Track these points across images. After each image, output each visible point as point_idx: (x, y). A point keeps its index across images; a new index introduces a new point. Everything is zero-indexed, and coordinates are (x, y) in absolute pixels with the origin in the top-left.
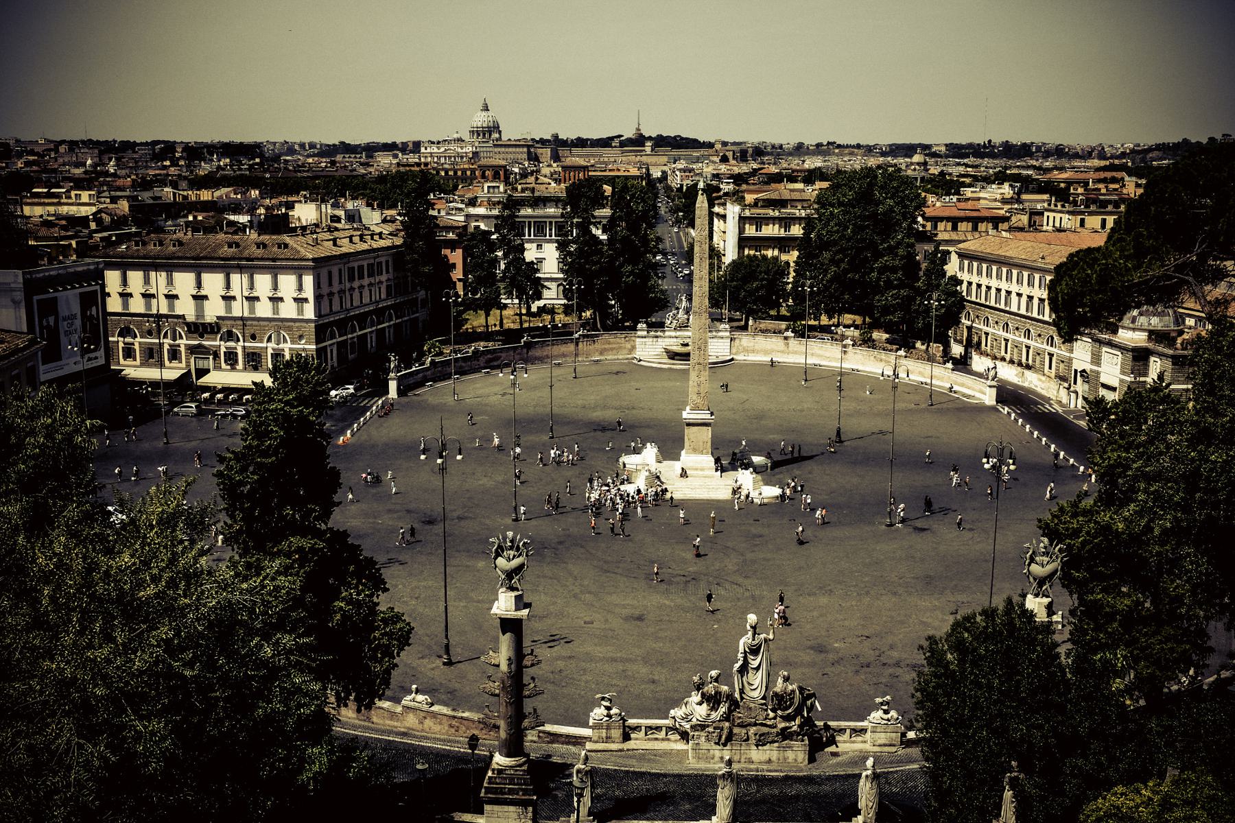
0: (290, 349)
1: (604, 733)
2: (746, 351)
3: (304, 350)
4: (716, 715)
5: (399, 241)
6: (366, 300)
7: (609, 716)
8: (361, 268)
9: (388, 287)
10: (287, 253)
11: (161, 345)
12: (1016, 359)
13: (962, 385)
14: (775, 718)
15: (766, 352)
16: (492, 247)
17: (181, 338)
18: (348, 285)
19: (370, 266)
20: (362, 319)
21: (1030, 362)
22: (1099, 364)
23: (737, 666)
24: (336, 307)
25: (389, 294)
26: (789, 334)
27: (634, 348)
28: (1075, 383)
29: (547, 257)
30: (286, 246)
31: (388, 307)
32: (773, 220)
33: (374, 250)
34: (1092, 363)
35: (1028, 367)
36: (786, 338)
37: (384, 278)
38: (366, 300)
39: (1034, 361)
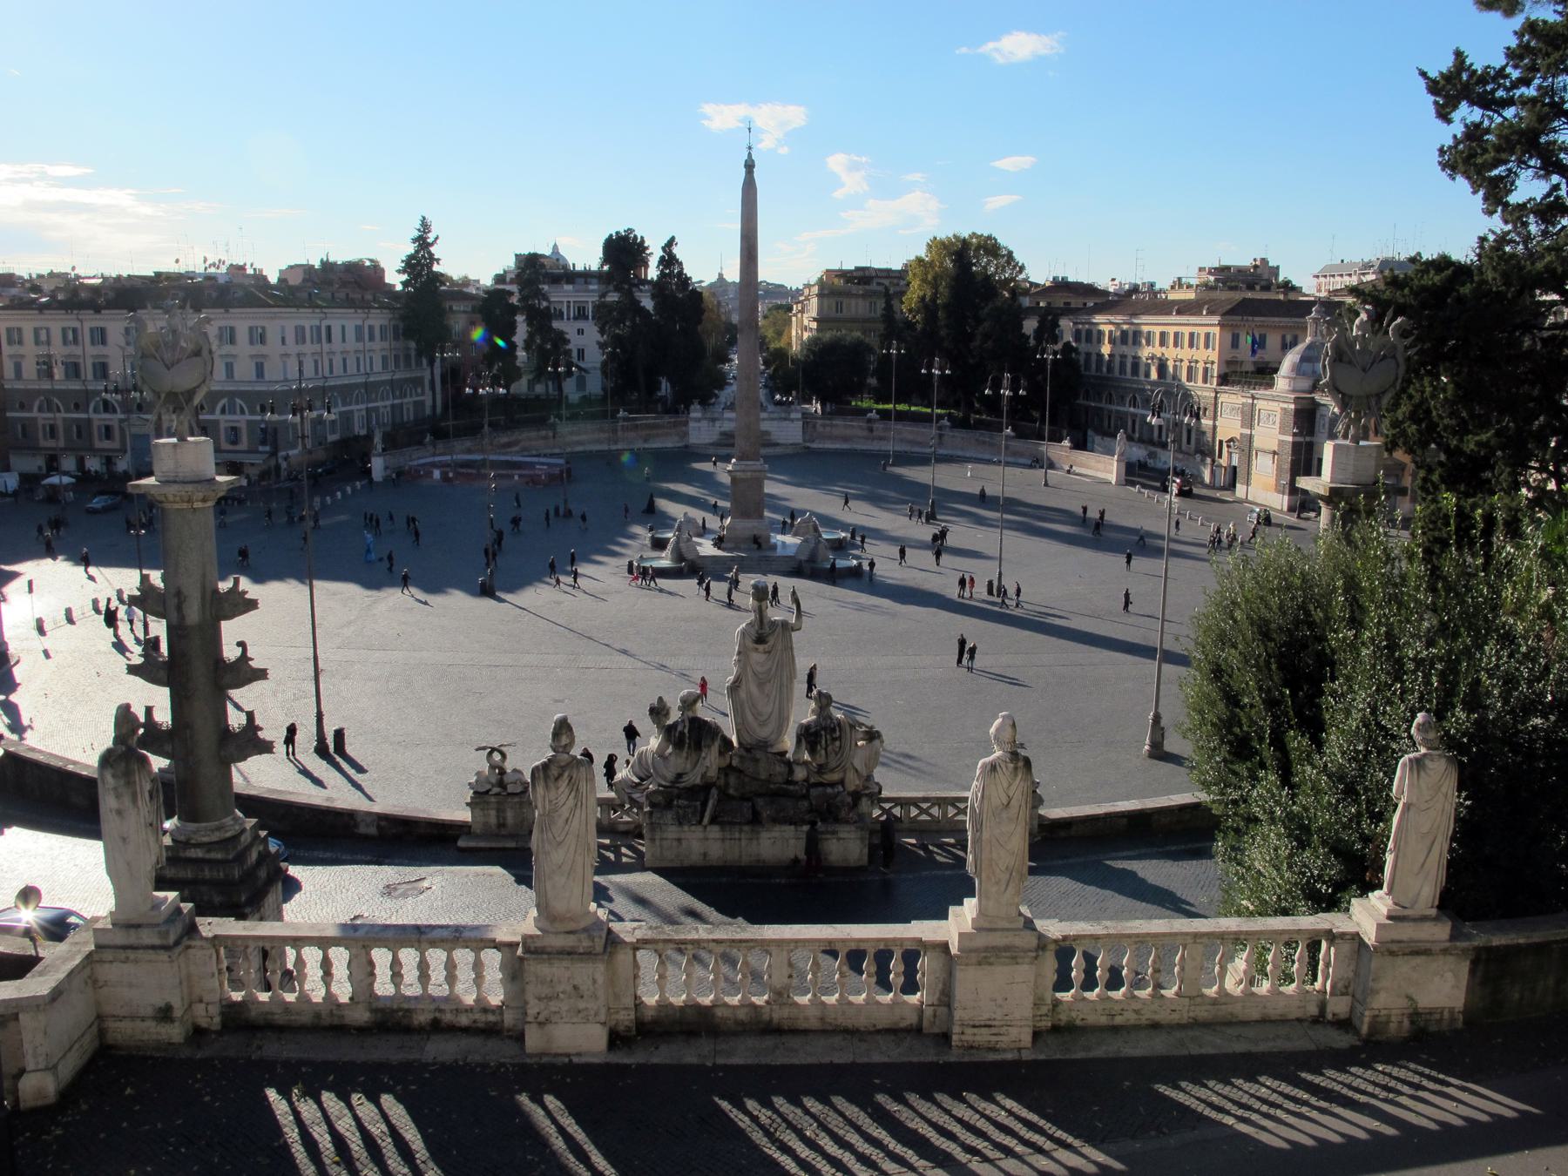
1: (493, 820)
4: (694, 778)
6: (352, 368)
7: (501, 784)
9: (384, 359)
11: (89, 421)
12: (1145, 437)
13: (1082, 465)
14: (806, 780)
15: (845, 439)
16: (514, 310)
17: (115, 411)
19: (359, 329)
20: (346, 392)
22: (1251, 427)
23: (731, 678)
25: (385, 366)
27: (686, 434)
29: (586, 340)
31: (383, 382)
32: (857, 296)
36: (869, 421)
38: (352, 368)
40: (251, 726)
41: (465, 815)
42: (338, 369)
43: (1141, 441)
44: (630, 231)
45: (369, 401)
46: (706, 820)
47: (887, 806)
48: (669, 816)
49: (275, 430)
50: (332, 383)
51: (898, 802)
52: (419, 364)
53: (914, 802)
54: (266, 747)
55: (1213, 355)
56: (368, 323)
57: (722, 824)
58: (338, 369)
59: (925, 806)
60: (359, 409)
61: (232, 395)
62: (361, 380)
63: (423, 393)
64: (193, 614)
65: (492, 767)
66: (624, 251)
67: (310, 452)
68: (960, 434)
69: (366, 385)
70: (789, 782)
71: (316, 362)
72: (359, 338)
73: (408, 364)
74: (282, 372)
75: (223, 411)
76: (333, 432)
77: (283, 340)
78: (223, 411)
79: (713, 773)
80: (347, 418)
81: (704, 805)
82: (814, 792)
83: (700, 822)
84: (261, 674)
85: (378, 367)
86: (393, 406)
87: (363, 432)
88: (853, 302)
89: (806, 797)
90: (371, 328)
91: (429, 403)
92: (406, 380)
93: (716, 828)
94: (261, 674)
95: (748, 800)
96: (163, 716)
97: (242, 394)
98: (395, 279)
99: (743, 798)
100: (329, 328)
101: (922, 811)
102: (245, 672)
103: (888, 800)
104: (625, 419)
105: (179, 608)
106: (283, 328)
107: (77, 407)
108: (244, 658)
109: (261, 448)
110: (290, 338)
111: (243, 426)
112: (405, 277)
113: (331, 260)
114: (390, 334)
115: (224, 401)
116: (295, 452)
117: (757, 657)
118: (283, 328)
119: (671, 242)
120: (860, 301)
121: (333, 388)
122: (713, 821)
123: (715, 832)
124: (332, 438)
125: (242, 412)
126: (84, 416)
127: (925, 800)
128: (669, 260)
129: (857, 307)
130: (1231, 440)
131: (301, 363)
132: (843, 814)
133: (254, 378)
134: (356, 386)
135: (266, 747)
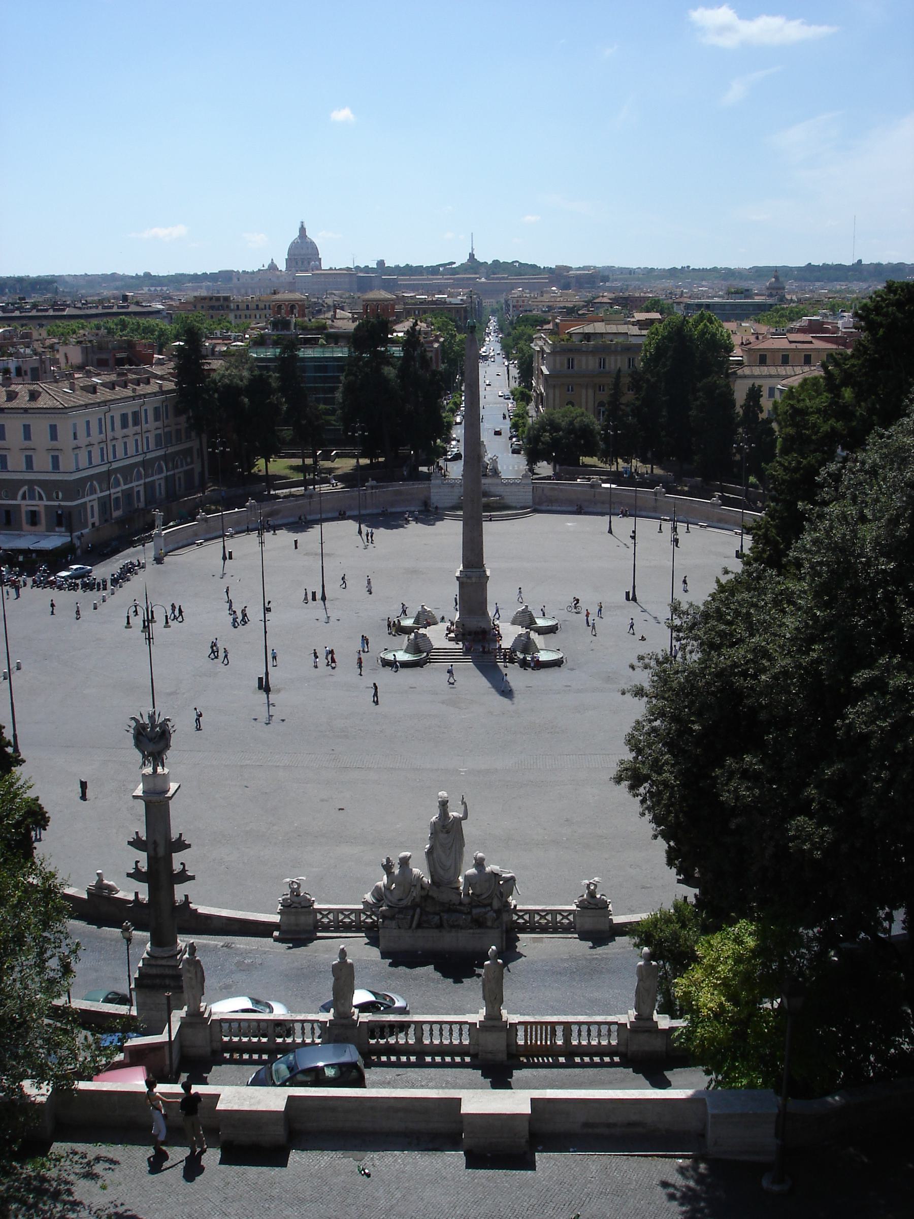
0: (46, 506)
3: (59, 506)
5: (170, 385)
8: (124, 417)
9: (158, 437)
10: (42, 403)
18: (110, 435)
20: (127, 472)
24: (96, 459)
33: (145, 396)
38: (131, 450)
41: (276, 918)
42: (120, 453)
45: (146, 476)
46: (414, 925)
47: (521, 914)
48: (393, 924)
49: (70, 514)
50: (115, 466)
57: (423, 928)
58: (120, 453)
60: (137, 485)
61: (31, 483)
62: (139, 459)
63: (192, 462)
64: (161, 851)
65: (292, 892)
67: (98, 529)
69: (144, 463)
71: (102, 449)
72: (136, 423)
74: (75, 465)
75: (24, 498)
76: (117, 508)
77: (75, 434)
78: (24, 498)
79: (418, 900)
80: (128, 494)
81: (413, 917)
82: (475, 911)
83: (410, 927)
86: (167, 478)
87: (142, 505)
88: (584, 359)
89: (470, 913)
92: (177, 453)
93: (420, 931)
94: (192, 878)
95: (438, 914)
96: (144, 897)
97: (42, 483)
99: (435, 914)
100: (112, 417)
101: (542, 917)
102: (183, 877)
103: (521, 911)
104: (372, 487)
105: (155, 849)
106: (75, 425)
108: (184, 870)
109: (57, 529)
110: (82, 433)
111: (42, 511)
115: (25, 488)
116: (87, 530)
117: (442, 836)
118: (75, 425)
121: (116, 470)
122: (419, 926)
123: (420, 933)
124: (116, 514)
125: (41, 498)
129: (588, 363)
131: (90, 452)
133: (50, 469)
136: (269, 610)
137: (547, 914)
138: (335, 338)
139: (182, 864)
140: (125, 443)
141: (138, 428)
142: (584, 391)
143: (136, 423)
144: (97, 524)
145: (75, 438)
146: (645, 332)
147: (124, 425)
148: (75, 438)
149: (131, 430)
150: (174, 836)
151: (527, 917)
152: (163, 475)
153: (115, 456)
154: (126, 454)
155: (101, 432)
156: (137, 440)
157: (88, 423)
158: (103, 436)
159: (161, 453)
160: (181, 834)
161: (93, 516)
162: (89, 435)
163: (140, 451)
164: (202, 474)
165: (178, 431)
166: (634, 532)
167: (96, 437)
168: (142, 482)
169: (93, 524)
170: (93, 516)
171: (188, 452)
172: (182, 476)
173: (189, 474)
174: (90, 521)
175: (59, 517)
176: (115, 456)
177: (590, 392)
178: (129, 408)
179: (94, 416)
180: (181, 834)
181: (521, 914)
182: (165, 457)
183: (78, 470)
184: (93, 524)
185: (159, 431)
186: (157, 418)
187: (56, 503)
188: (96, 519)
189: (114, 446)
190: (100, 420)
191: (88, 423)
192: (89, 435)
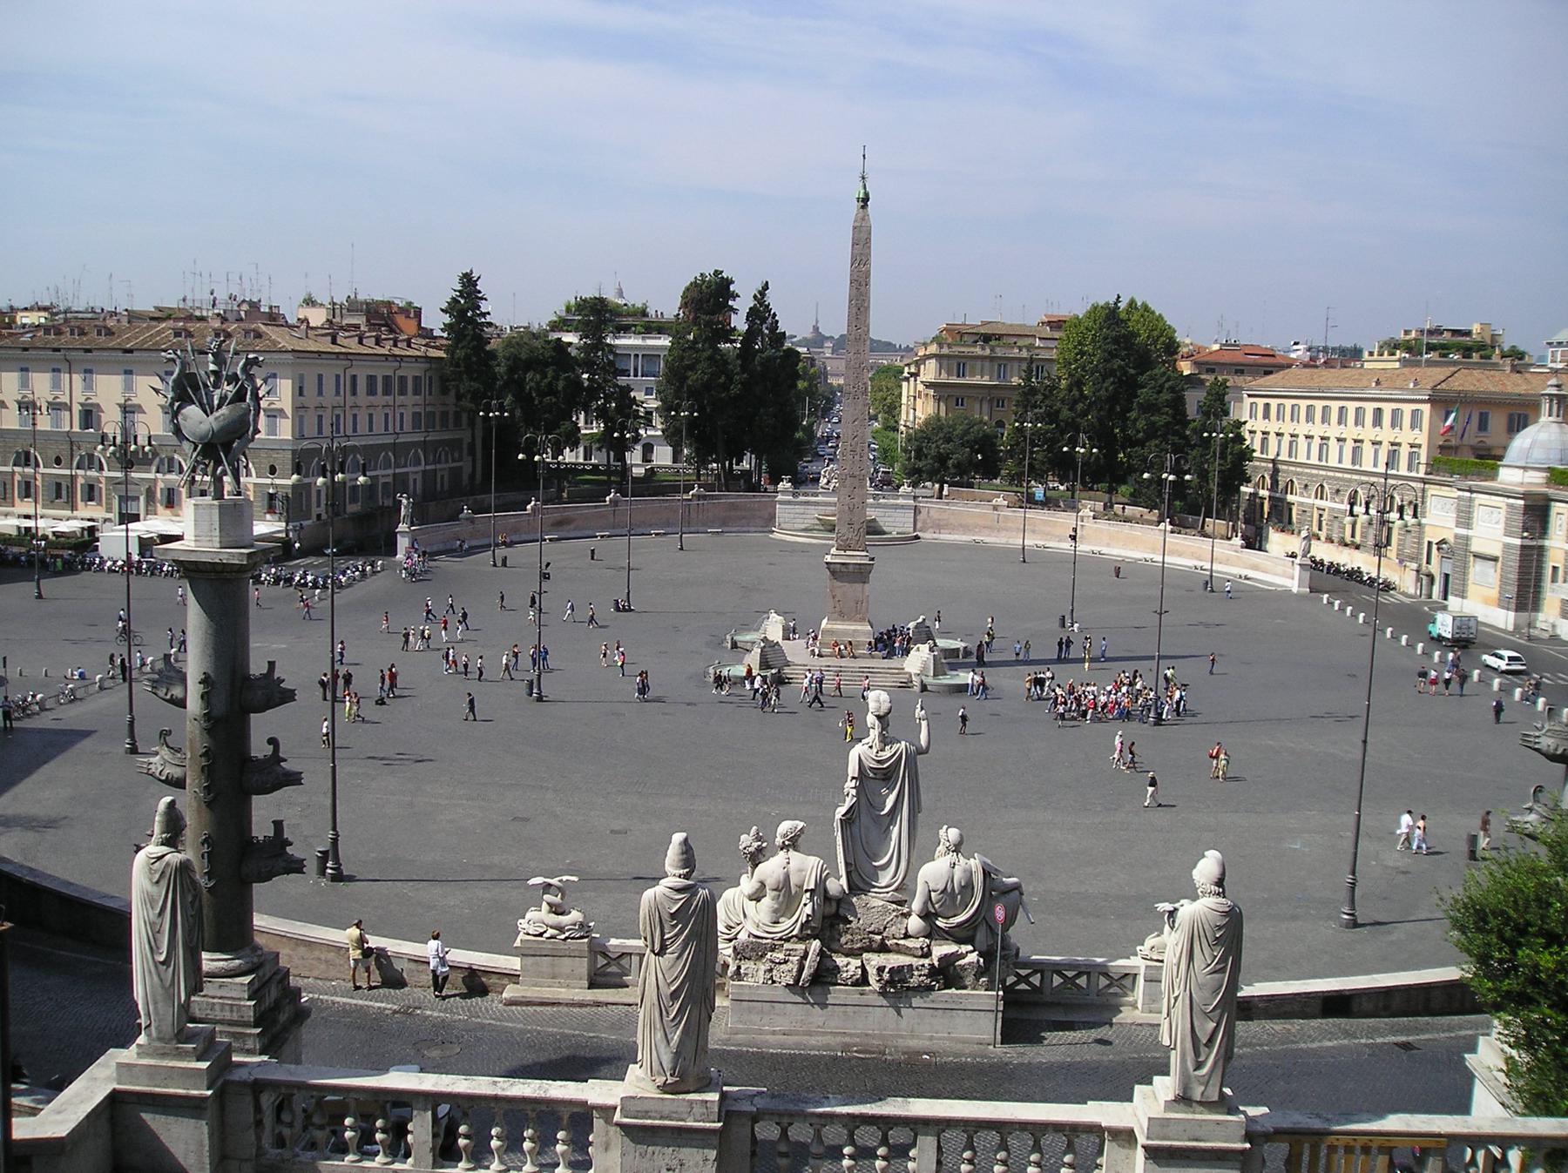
2: (938, 527)
6: (379, 426)
8: (371, 380)
9: (414, 414)
20: (371, 452)
21: (1358, 539)
22: (1468, 526)
26: (1000, 501)
28: (1428, 562)
30: (259, 335)
31: (414, 444)
34: (1458, 524)
35: (1357, 547)
36: (995, 508)
37: (410, 399)
38: (379, 426)
39: (1364, 536)
40: (279, 841)
41: (513, 963)
42: (363, 427)
43: (1330, 540)
44: (717, 273)
45: (397, 466)
47: (1023, 972)
51: (1039, 968)
52: (457, 423)
53: (1057, 969)
54: (296, 867)
55: (1422, 437)
56: (399, 373)
58: (363, 427)
59: (1070, 974)
62: (389, 440)
63: (460, 459)
66: (710, 296)
67: (325, 524)
68: (1103, 525)
69: (394, 447)
70: (907, 936)
73: (444, 424)
76: (354, 500)
82: (941, 950)
84: (294, 779)
85: (407, 427)
86: (424, 472)
90: (403, 379)
91: (467, 470)
98: (436, 320)
100: (354, 378)
104: (699, 497)
107: (58, 461)
108: (276, 758)
112: (447, 319)
113: (361, 297)
114: (424, 387)
119: (766, 287)
120: (987, 364)
124: (352, 508)
126: (68, 472)
127: (1071, 966)
128: (760, 313)
130: (1443, 541)
132: (969, 980)
134: (383, 447)
135: (296, 867)
136: (546, 576)
137: (1079, 975)
138: (658, 328)
139: (273, 741)
140: (371, 415)
141: (389, 399)
142: (977, 406)
143: (387, 392)
144: (324, 516)
145: (301, 394)
146: (1057, 335)
147: (371, 391)
148: (301, 394)
149: (380, 399)
150: (257, 668)
151: (1036, 980)
152: (422, 468)
153: (355, 430)
154: (371, 429)
155: (338, 393)
156: (387, 415)
157: (320, 377)
158: (340, 399)
159: (419, 438)
160: (272, 665)
161: (319, 506)
162: (320, 393)
163: (391, 430)
164: (472, 476)
165: (445, 414)
166: (1075, 530)
167: (329, 397)
168: (390, 472)
169: (319, 516)
170: (319, 506)
171: (454, 445)
172: (446, 474)
173: (455, 473)
174: (315, 511)
175: (272, 497)
176: (355, 430)
177: (986, 407)
178: (380, 371)
179: (330, 372)
180: (272, 665)
181: (1023, 972)
182: (424, 445)
183: (302, 437)
184: (319, 516)
185: (417, 409)
186: (416, 392)
187: (269, 481)
188: (322, 510)
189: (355, 416)
190: (338, 377)
191: (320, 377)
192: (320, 393)
